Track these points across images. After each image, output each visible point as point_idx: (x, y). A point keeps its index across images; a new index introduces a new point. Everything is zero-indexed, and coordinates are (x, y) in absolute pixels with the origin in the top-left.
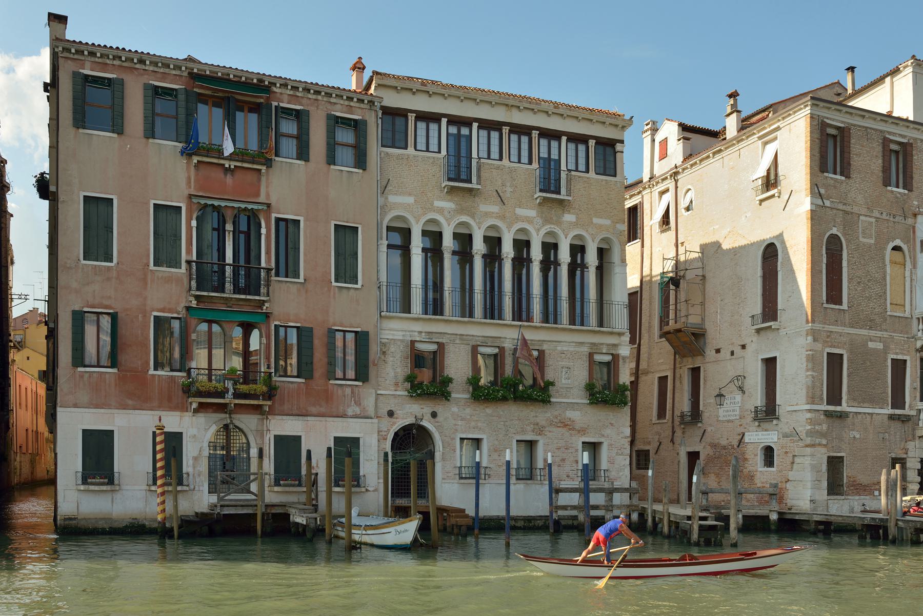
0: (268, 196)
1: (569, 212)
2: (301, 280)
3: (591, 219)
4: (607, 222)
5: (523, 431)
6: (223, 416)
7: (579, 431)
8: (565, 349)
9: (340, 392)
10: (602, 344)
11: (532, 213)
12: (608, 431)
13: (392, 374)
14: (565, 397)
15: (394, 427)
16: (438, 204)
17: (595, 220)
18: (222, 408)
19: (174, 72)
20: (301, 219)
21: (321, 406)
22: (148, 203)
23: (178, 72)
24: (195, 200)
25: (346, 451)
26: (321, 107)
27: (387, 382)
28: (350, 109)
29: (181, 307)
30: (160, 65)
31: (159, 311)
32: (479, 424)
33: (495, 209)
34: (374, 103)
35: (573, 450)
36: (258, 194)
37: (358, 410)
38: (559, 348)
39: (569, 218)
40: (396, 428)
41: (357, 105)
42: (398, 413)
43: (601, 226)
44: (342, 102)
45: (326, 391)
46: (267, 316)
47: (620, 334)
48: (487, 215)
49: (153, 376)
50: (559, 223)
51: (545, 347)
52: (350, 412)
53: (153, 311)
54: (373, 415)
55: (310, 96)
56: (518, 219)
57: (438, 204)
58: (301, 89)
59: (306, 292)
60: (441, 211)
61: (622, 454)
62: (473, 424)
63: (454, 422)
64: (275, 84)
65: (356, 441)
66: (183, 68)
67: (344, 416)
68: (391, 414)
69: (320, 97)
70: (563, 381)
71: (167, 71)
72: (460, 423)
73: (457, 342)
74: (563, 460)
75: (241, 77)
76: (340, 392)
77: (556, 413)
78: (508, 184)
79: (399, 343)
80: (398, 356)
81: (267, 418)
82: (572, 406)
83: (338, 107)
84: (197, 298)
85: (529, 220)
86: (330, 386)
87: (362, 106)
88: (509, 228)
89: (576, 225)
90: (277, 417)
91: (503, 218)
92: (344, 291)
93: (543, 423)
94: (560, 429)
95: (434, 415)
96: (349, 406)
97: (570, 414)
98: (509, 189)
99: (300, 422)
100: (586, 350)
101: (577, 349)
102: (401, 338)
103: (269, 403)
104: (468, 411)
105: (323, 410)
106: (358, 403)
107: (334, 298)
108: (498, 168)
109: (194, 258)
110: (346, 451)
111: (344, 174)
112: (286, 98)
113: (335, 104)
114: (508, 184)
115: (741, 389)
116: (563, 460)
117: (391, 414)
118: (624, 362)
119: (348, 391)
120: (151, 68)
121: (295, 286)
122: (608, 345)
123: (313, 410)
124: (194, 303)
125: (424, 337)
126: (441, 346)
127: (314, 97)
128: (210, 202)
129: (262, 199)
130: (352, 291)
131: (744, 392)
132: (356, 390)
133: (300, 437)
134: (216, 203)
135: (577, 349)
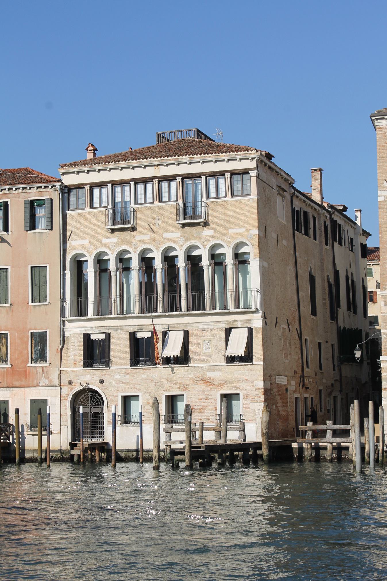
2: (9, 305)
3: (227, 231)
4: (242, 230)
5: (171, 389)
7: (217, 386)
8: (205, 327)
9: (34, 371)
10: (237, 321)
12: (243, 385)
13: (72, 357)
14: (206, 362)
15: (72, 391)
16: (105, 241)
17: (231, 231)
21: (22, 381)
26: (21, 197)
27: (69, 362)
32: (136, 386)
33: (147, 237)
34: (55, 186)
35: (213, 400)
37: (47, 382)
38: (201, 327)
39: (207, 232)
40: (74, 392)
42: (76, 381)
45: (26, 371)
50: (198, 238)
51: (188, 328)
52: (41, 384)
54: (57, 385)
55: (14, 192)
56: (165, 241)
57: (105, 241)
60: (107, 245)
61: (257, 402)
62: (131, 386)
63: (116, 385)
67: (37, 386)
70: (205, 351)
72: (121, 385)
73: (120, 331)
74: (204, 408)
76: (34, 371)
77: (199, 374)
78: (157, 218)
79: (77, 336)
80: (76, 345)
82: (213, 368)
85: (174, 240)
86: (28, 368)
88: (158, 249)
91: (153, 242)
92: (37, 307)
93: (188, 382)
94: (202, 386)
95: (102, 381)
96: (40, 380)
97: (210, 374)
98: (157, 222)
100: (224, 326)
101: (216, 326)
102: (79, 332)
104: (128, 377)
105: (23, 383)
106: (47, 378)
107: (31, 313)
114: (157, 218)
116: (204, 408)
117: (70, 383)
118: (257, 333)
119: (40, 370)
121: (5, 309)
122: (242, 321)
125: (94, 330)
126: (108, 335)
130: (43, 306)
132: (45, 368)
133: (8, 401)
135: (216, 326)
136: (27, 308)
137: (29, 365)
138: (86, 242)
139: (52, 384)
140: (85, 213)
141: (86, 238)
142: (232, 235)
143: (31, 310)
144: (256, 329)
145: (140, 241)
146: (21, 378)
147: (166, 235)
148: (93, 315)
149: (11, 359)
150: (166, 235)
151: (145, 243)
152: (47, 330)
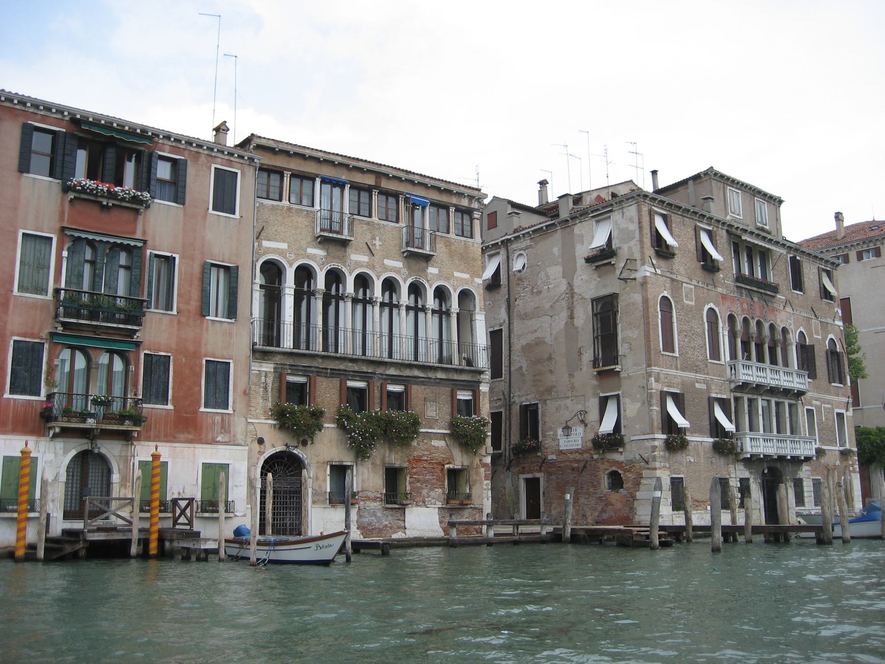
0: (144, 233)
1: (433, 266)
6: (85, 441)
11: (399, 264)
17: (456, 274)
18: (84, 433)
19: (55, 116)
20: (177, 256)
21: (189, 433)
22: (15, 233)
23: (59, 116)
24: (68, 233)
25: (215, 474)
28: (230, 163)
29: (45, 333)
30: (42, 108)
31: (18, 335)
33: (365, 259)
36: (134, 232)
39: (432, 270)
40: (267, 455)
41: (238, 160)
43: (462, 279)
44: (222, 156)
46: (138, 344)
47: (481, 372)
48: (358, 264)
49: (9, 399)
53: (14, 335)
56: (386, 269)
58: (183, 142)
59: (179, 322)
64: (158, 136)
65: (225, 467)
66: (66, 113)
67: (214, 442)
68: (261, 441)
69: (201, 151)
71: (48, 114)
75: (124, 127)
76: (210, 421)
78: (377, 238)
81: (132, 444)
83: (219, 160)
84: (64, 324)
85: (398, 271)
87: (242, 161)
89: (439, 277)
90: (142, 443)
91: (373, 267)
92: (218, 324)
98: (377, 243)
99: (167, 449)
103: (138, 429)
105: (191, 437)
107: (207, 330)
108: (368, 223)
109: (63, 286)
110: (215, 474)
111: (222, 220)
112: (167, 148)
113: (215, 157)
115: (582, 421)
119: (218, 418)
120: (31, 110)
121: (168, 318)
123: (182, 436)
124: (60, 329)
127: (196, 150)
128: (84, 236)
129: (138, 235)
130: (225, 324)
131: (586, 425)
134: (91, 237)
136: (202, 323)
137: (202, 409)
138: (284, 246)
139: (236, 442)
140: (283, 207)
141: (284, 242)
142: (457, 279)
143: (207, 327)
144: (484, 393)
145: (356, 262)
146: (186, 426)
147: (387, 262)
148: (321, 349)
149: (173, 397)
150: (387, 262)
151: (362, 266)
152: (231, 361)
